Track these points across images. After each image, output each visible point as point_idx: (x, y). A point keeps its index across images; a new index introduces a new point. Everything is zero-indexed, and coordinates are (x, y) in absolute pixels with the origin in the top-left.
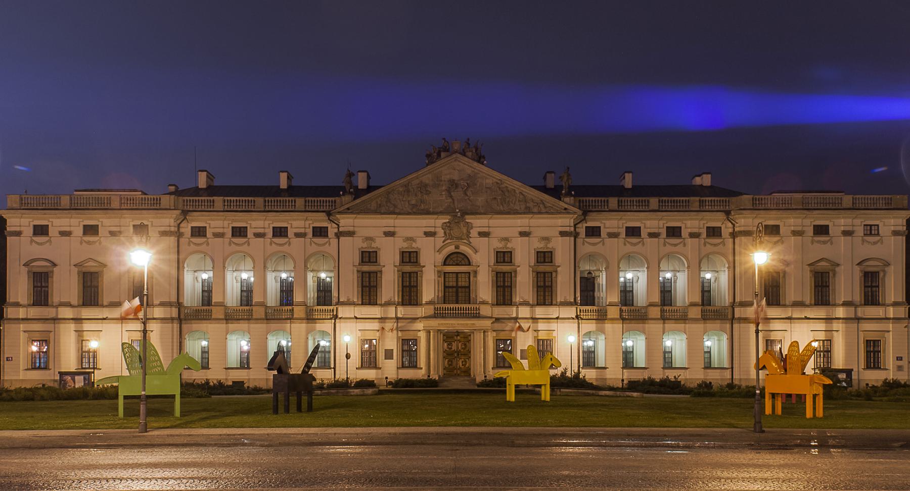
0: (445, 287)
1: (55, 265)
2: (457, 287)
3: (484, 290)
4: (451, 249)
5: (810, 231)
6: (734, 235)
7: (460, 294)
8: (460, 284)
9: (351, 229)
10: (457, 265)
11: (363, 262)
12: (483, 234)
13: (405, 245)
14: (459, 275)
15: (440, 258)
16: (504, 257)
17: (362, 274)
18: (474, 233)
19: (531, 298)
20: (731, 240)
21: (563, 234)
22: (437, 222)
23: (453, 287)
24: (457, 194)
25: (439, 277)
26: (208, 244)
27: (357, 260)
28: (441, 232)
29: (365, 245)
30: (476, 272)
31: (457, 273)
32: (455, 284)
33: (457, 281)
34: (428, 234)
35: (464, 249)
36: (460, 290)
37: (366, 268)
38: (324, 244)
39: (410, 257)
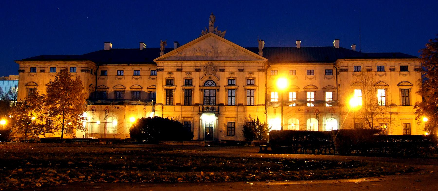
0: (204, 97)
2: (210, 97)
3: (223, 98)
4: (207, 78)
5: (398, 69)
6: (337, 74)
11: (167, 85)
13: (186, 76)
14: (211, 91)
15: (202, 83)
17: (185, 90)
19: (164, 102)
23: (208, 97)
27: (164, 83)
30: (218, 90)
31: (210, 90)
32: (209, 95)
33: (210, 94)
35: (214, 78)
37: (168, 88)
39: (188, 82)
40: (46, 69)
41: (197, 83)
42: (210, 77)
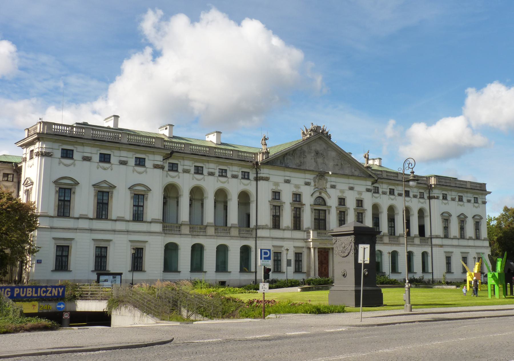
1: (77, 183)
7: (321, 224)
8: (321, 218)
9: (268, 176)
10: (319, 205)
12: (333, 187)
14: (321, 212)
16: (342, 201)
18: (328, 185)
20: (428, 200)
21: (368, 190)
22: (310, 177)
24: (320, 160)
25: (312, 212)
26: (179, 178)
28: (313, 184)
29: (274, 188)
34: (307, 184)
35: (324, 195)
36: (321, 221)
38: (248, 185)
40: (54, 151)
41: (308, 200)
42: (320, 193)
